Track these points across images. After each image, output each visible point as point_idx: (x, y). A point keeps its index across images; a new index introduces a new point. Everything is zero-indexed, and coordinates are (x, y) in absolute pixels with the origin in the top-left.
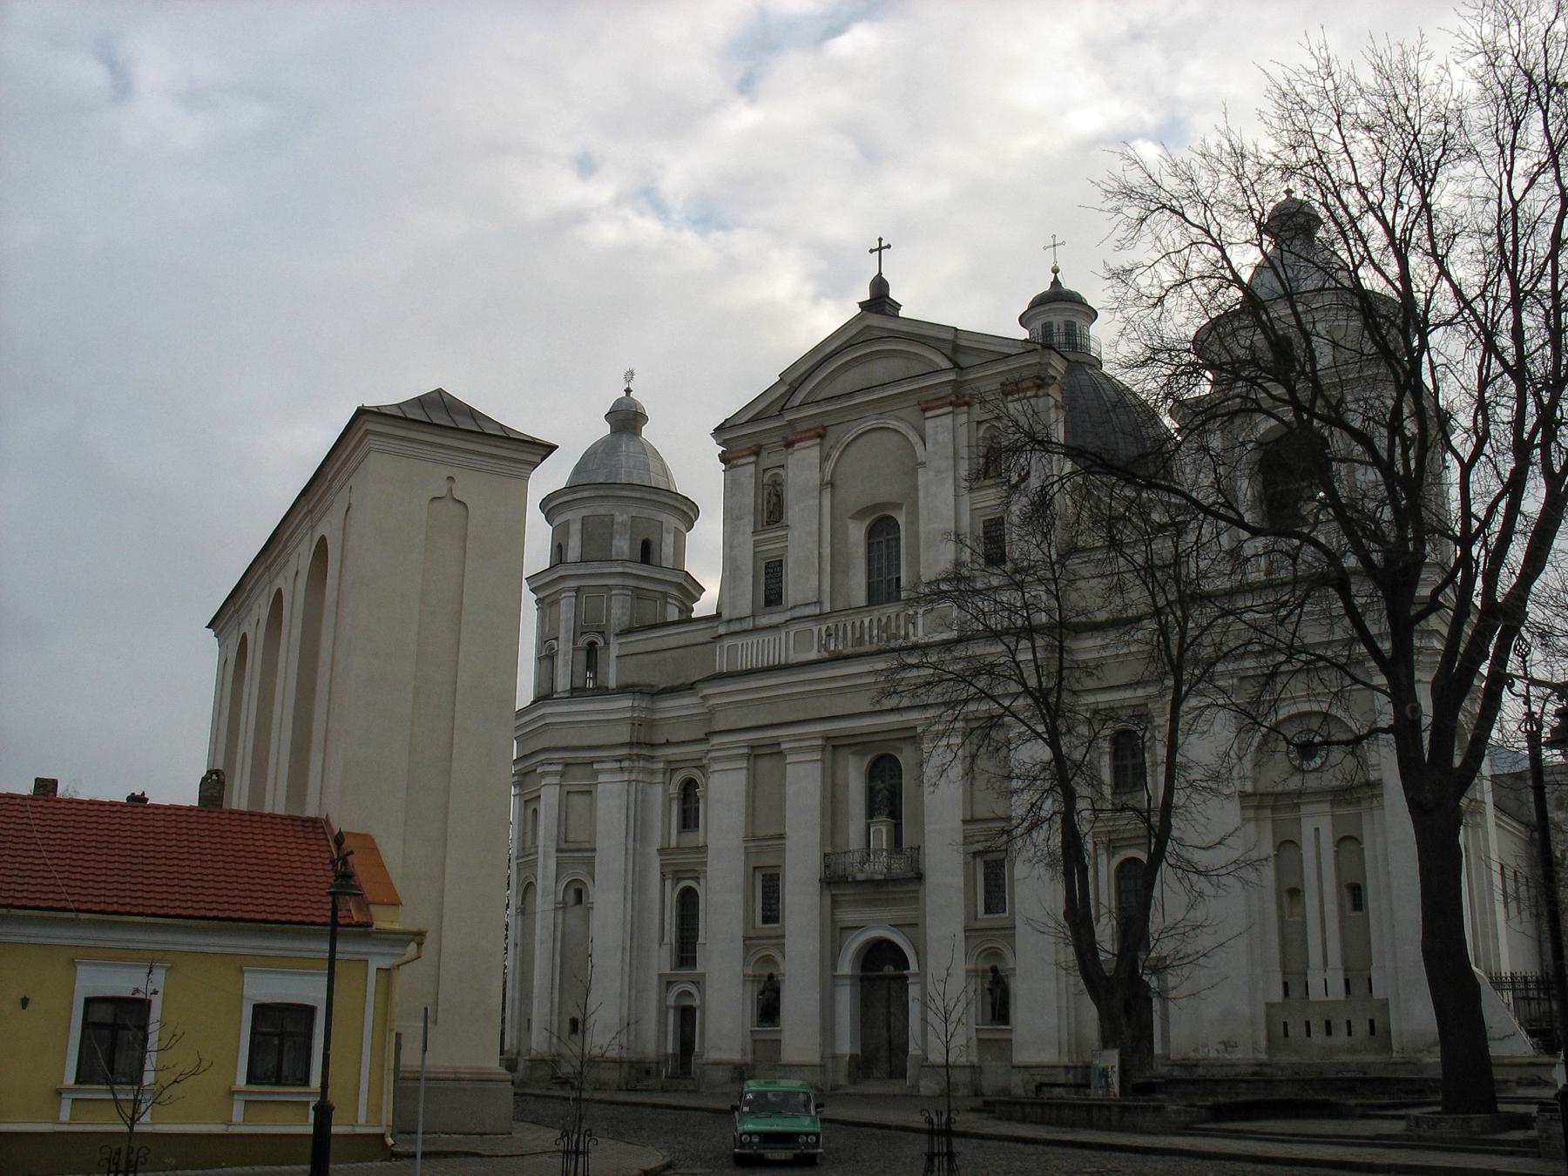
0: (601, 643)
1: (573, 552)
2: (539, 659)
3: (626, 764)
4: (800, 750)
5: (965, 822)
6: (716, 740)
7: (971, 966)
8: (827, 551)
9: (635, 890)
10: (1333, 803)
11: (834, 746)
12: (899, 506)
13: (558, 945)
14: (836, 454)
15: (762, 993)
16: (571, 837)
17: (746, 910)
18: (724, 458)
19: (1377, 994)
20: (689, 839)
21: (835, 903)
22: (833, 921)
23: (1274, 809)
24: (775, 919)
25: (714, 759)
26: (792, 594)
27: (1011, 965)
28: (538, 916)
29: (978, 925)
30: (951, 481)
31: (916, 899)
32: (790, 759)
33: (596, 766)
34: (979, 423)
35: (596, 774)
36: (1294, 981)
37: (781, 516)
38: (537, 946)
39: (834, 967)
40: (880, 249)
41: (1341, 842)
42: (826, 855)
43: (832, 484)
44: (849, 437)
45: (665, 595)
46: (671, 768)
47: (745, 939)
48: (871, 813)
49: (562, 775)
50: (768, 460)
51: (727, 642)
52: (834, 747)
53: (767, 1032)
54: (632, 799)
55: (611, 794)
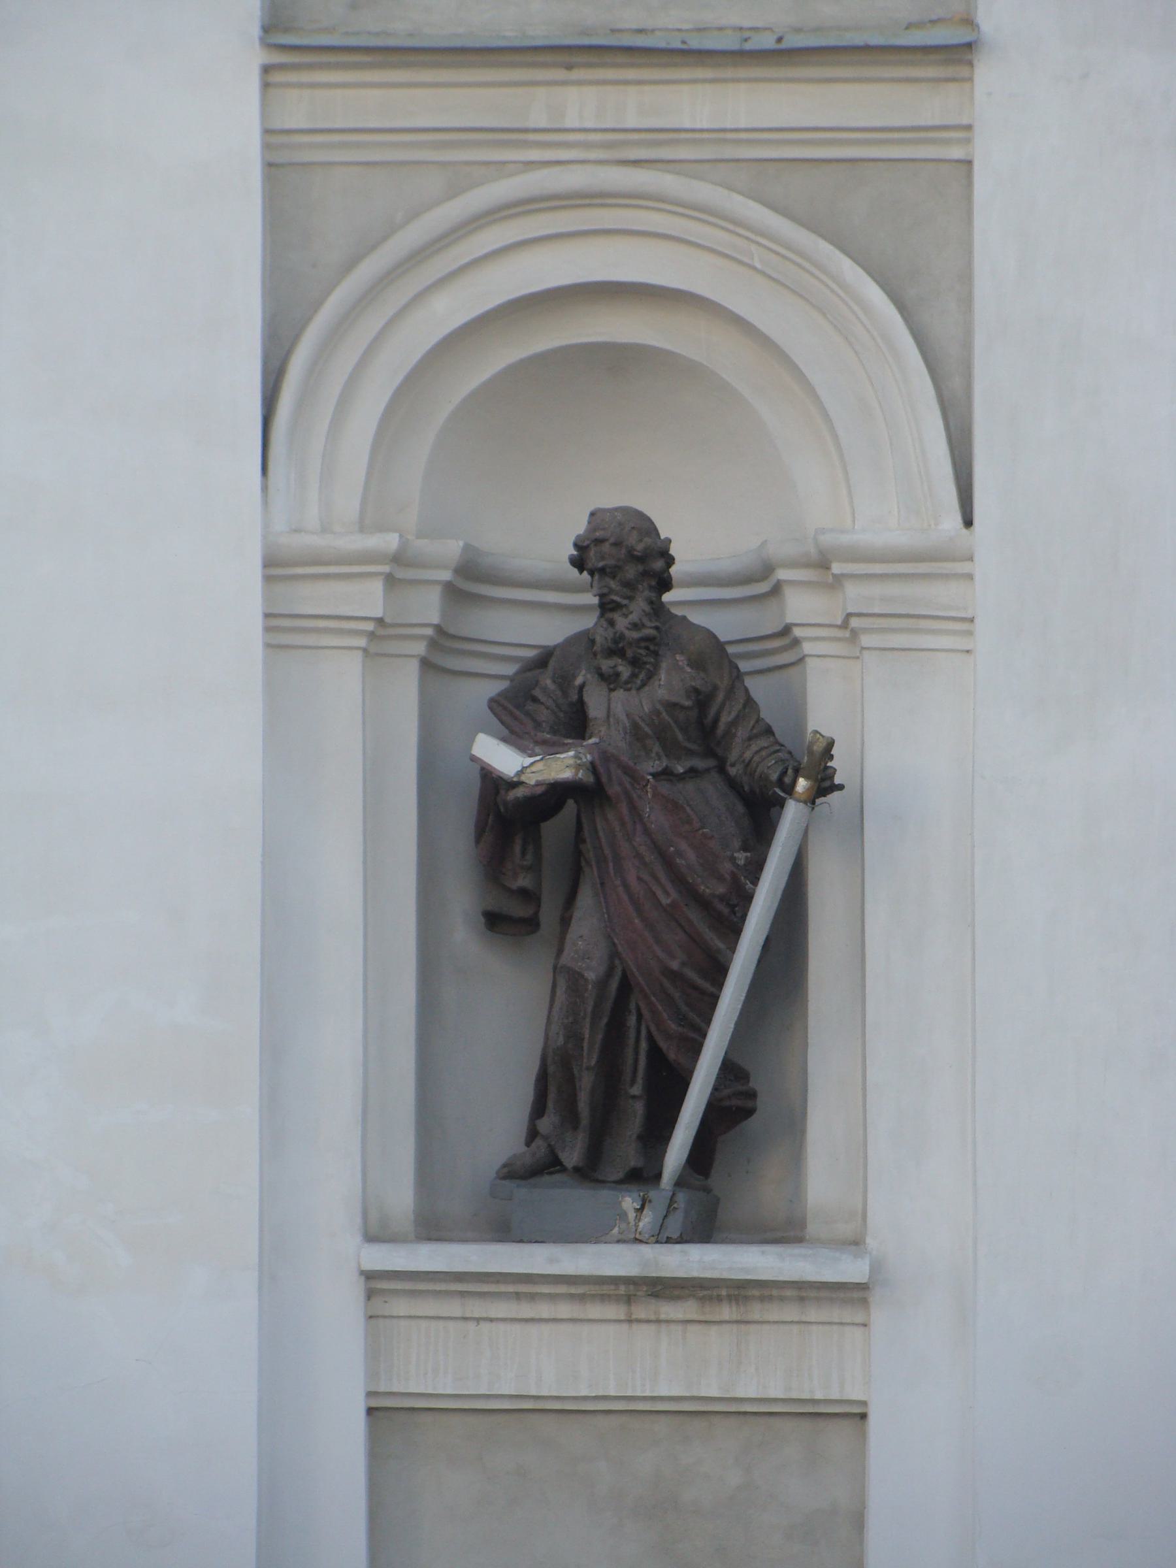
7: (334, 500)
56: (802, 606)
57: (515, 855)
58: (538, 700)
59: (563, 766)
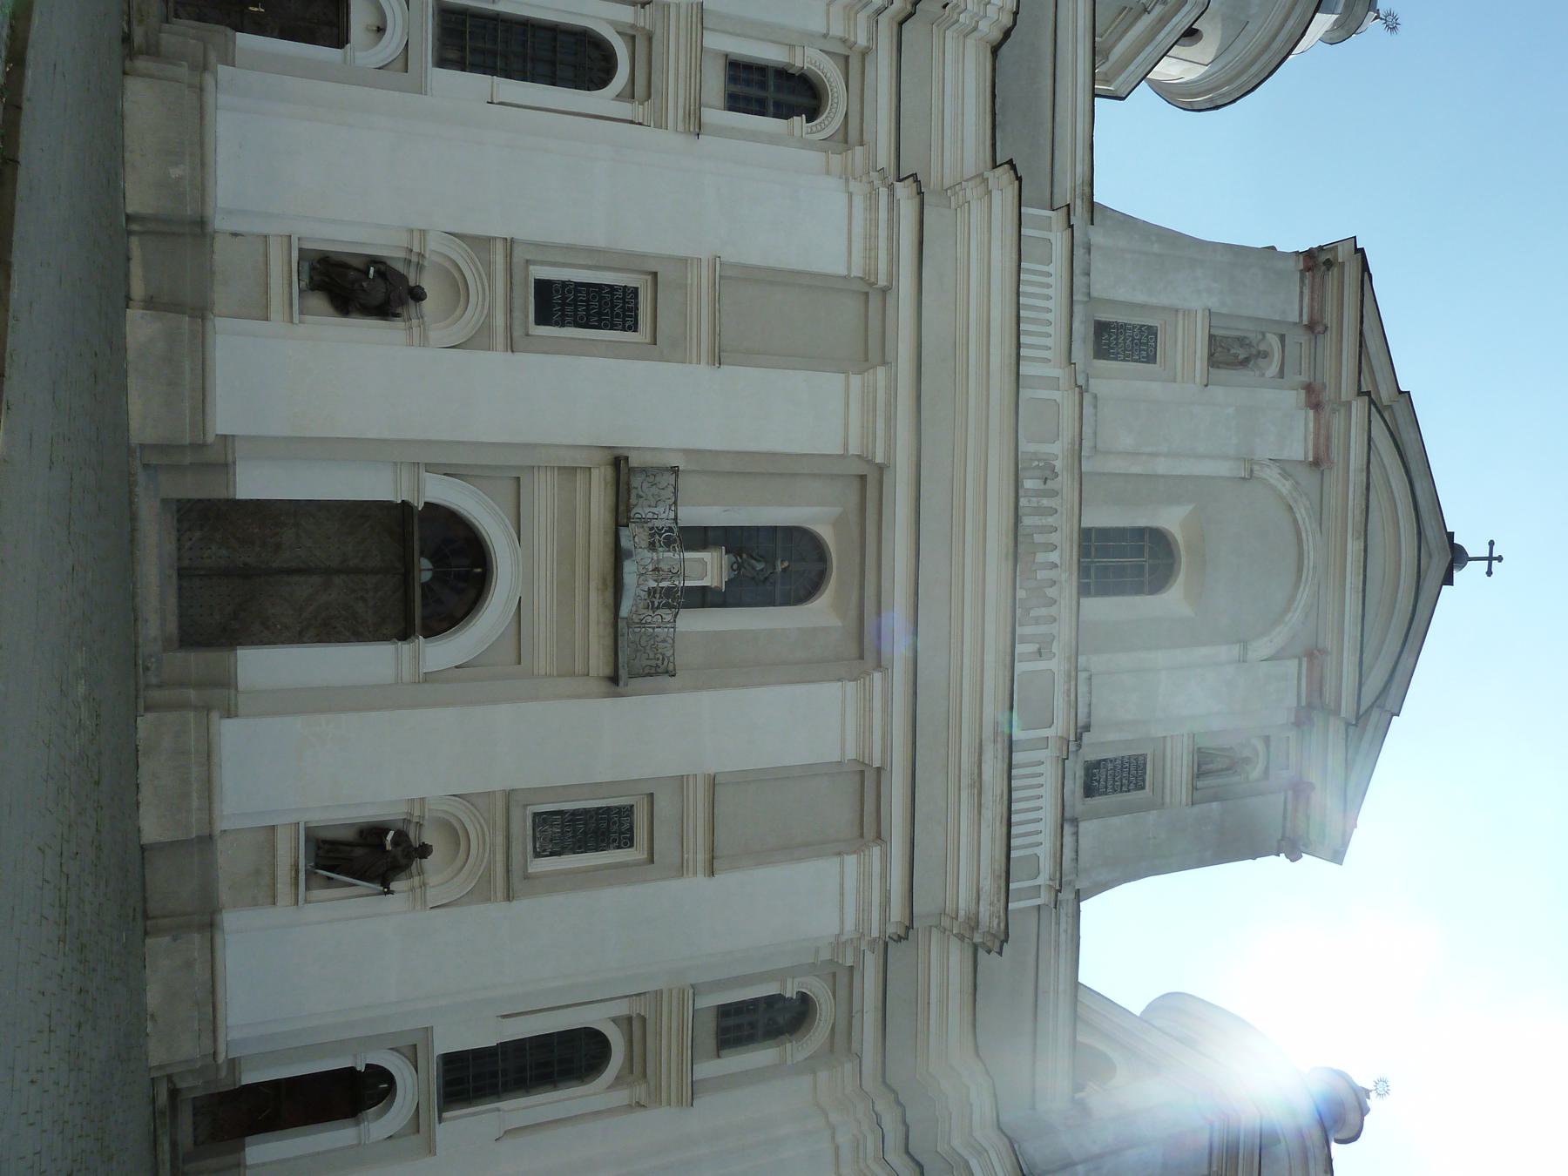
8: (1162, 467)
11: (866, 483)
14: (1285, 487)
18: (1310, 255)
20: (715, 83)
24: (543, 317)
25: (872, 197)
27: (434, 895)
29: (516, 813)
32: (856, 381)
39: (430, 468)
42: (675, 470)
44: (1301, 514)
47: (510, 244)
48: (732, 539)
50: (1297, 338)
51: (1059, 239)
52: (863, 478)
53: (282, 275)
56: (416, 880)
57: (372, 834)
58: (401, 836)
59: (389, 847)
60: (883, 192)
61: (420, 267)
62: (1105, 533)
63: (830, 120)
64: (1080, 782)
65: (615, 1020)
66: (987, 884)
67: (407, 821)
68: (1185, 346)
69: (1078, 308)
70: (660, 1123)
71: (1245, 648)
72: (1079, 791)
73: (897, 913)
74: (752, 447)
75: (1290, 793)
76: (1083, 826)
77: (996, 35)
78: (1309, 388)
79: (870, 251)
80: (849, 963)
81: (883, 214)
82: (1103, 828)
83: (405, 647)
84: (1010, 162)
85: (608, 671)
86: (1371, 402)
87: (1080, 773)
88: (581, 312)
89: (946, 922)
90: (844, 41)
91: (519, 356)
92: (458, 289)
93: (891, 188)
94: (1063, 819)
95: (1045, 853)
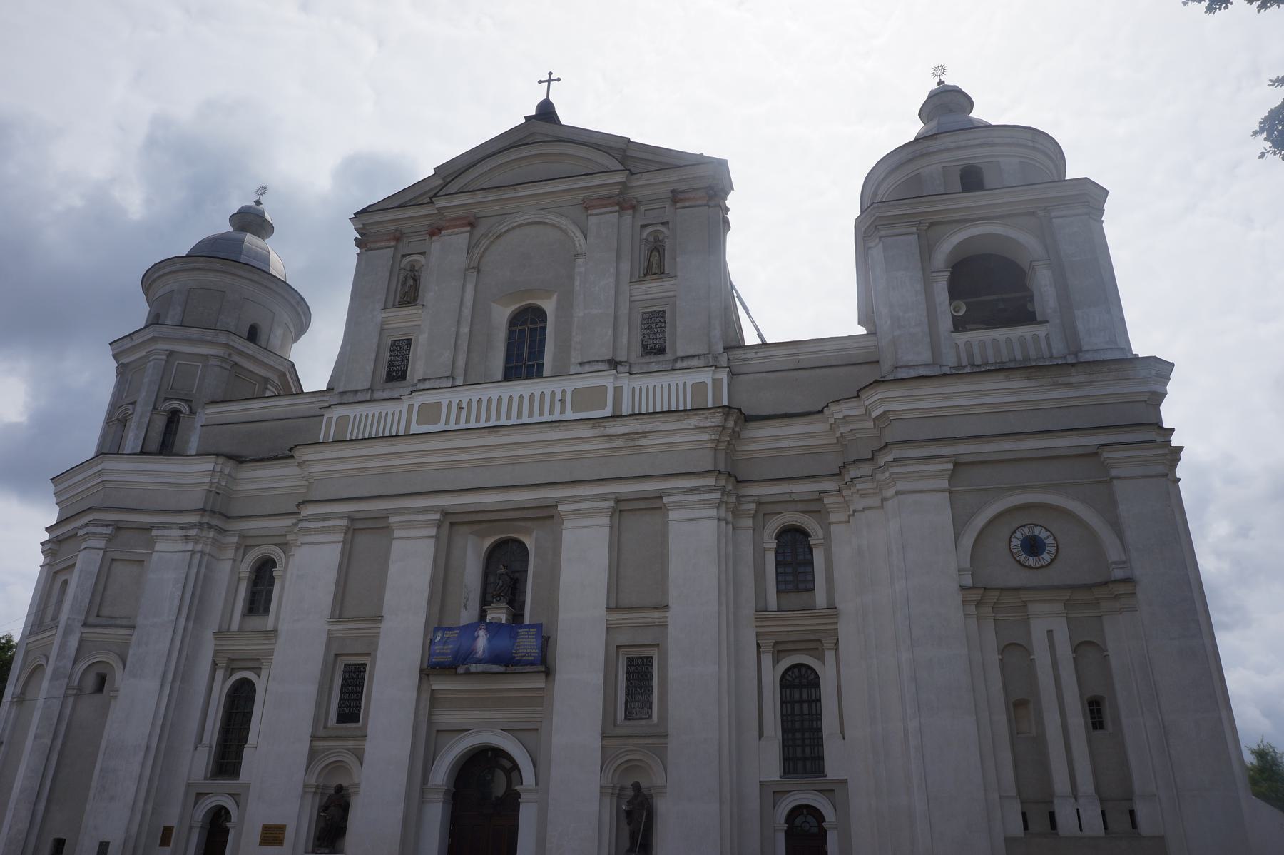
0: (184, 408)
1: (173, 316)
2: (109, 421)
3: (193, 532)
4: (411, 525)
5: (608, 609)
6: (308, 511)
8: (465, 329)
9: (180, 676)
10: (1068, 604)
11: (452, 522)
12: (547, 293)
13: (59, 741)
14: (485, 243)
15: (325, 808)
16: (106, 611)
17: (318, 705)
18: (358, 243)
19: (1145, 827)
20: (255, 622)
21: (434, 700)
22: (430, 722)
23: (995, 607)
24: (354, 718)
25: (307, 531)
26: (417, 368)
28: (40, 703)
30: (613, 270)
31: (541, 701)
32: (397, 534)
33: (154, 532)
34: (644, 226)
35: (151, 543)
36: (1039, 814)
37: (416, 299)
38: (29, 743)
39: (425, 780)
40: (549, 81)
41: (1079, 648)
43: (479, 272)
45: (266, 380)
46: (246, 544)
47: (314, 737)
49: (110, 539)
51: (337, 412)
52: (452, 524)
54: (194, 571)
55: (169, 562)
60: (300, 525)
61: (325, 787)
62: (508, 358)
63: (277, 553)
64: (654, 359)
65: (776, 661)
66: (693, 421)
67: (619, 796)
68: (402, 320)
69: (378, 395)
70: (847, 630)
71: (577, 255)
72: (660, 358)
73: (710, 481)
74: (426, 594)
75: (679, 205)
76: (680, 354)
77: (231, 463)
78: (432, 234)
79: (333, 530)
80: (753, 506)
81: (312, 525)
82: (682, 340)
83: (524, 797)
84: (291, 450)
85: (543, 676)
86: (435, 195)
87: (647, 359)
88: (354, 696)
89: (722, 446)
90: (237, 549)
91: (369, 732)
92: (338, 766)
93: (300, 521)
94: (673, 370)
95: (691, 378)
